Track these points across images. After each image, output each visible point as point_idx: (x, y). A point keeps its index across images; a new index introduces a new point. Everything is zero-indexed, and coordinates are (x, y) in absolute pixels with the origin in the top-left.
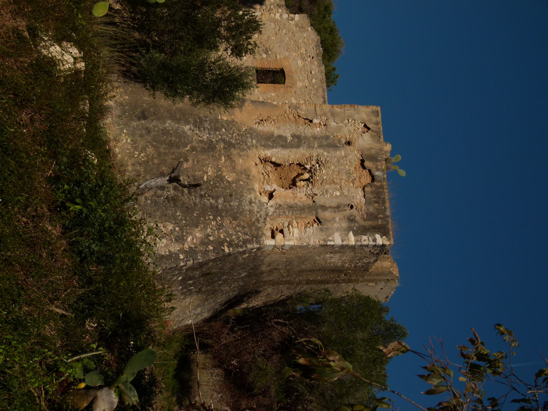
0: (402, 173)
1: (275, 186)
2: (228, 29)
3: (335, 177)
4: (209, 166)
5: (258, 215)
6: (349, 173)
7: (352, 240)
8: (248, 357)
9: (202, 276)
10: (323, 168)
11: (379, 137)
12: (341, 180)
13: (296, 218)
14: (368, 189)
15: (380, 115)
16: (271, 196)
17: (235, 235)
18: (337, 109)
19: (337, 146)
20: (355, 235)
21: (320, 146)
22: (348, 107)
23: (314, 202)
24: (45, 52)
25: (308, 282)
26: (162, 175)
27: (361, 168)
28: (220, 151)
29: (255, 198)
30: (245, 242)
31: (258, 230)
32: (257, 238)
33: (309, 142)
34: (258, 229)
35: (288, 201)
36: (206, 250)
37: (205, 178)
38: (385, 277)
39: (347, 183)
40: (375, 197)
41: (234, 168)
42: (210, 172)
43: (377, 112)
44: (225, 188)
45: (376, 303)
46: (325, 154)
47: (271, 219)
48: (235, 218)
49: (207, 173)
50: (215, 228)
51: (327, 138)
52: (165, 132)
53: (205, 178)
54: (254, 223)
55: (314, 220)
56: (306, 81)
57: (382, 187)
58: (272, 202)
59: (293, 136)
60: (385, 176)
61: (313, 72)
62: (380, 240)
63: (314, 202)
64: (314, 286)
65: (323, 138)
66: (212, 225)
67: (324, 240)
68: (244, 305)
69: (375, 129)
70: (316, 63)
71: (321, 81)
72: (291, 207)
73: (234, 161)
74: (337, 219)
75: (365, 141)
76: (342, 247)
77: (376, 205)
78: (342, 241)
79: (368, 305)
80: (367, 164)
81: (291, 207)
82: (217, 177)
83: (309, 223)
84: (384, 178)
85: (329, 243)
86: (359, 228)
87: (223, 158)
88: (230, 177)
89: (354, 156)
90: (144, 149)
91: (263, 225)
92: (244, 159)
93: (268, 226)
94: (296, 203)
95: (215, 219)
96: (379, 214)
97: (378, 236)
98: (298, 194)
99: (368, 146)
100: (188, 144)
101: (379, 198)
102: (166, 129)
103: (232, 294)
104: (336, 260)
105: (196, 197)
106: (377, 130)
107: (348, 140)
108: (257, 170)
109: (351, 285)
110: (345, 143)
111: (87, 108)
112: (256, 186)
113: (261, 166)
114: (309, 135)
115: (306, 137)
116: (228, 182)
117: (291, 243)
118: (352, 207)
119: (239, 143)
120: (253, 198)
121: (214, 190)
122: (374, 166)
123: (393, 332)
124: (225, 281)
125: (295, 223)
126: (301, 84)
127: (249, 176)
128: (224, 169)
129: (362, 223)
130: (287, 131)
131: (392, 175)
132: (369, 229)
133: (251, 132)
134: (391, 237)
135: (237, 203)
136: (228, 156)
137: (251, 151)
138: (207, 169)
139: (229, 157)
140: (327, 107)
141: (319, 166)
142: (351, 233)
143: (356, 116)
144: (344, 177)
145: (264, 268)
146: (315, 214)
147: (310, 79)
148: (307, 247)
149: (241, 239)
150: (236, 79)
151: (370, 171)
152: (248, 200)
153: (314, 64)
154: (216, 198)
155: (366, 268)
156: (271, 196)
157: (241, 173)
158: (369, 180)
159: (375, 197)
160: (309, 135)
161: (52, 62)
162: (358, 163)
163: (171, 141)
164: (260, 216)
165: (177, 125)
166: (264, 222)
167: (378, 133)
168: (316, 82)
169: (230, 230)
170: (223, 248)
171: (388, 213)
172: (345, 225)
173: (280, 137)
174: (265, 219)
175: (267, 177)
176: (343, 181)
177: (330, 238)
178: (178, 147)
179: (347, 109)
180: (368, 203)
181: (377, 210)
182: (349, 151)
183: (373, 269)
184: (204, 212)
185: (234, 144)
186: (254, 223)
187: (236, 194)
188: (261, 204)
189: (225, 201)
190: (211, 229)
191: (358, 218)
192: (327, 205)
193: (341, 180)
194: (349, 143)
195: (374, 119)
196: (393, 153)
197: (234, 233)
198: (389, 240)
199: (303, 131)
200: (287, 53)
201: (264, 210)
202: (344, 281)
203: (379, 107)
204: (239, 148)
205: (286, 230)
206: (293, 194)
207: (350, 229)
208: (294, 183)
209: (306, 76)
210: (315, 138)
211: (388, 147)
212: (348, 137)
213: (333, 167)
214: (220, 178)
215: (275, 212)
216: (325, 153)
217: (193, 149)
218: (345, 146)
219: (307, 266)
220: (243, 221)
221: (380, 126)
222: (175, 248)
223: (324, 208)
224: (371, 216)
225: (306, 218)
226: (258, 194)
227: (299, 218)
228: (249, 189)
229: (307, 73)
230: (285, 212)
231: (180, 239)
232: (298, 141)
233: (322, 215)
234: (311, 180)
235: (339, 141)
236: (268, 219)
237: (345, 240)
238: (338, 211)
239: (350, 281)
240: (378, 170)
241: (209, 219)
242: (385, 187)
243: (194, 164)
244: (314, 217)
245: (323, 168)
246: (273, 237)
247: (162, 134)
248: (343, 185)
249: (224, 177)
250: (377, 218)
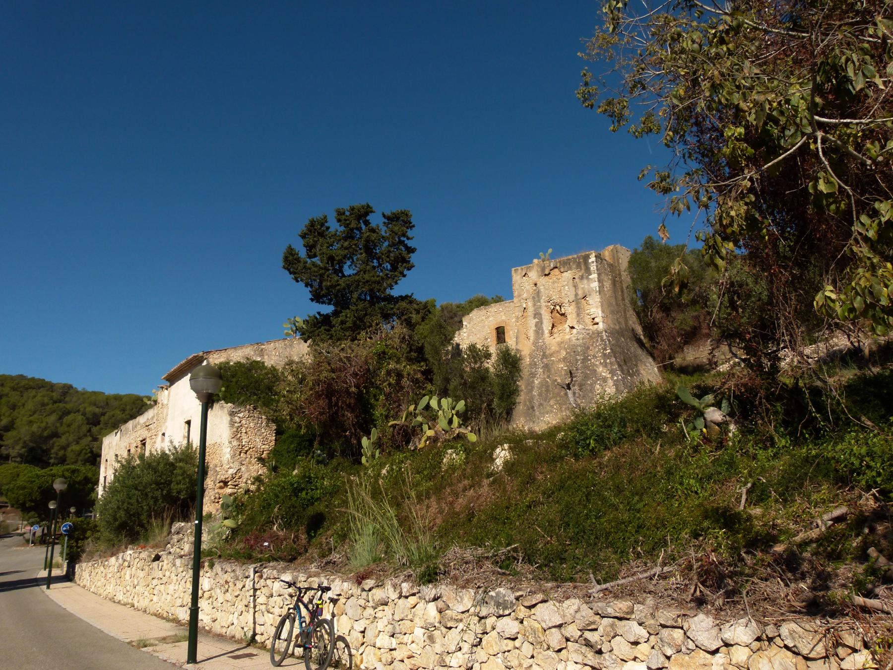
0: (550, 251)
1: (566, 326)
2: (476, 362)
6: (554, 283)
7: (594, 276)
8: (675, 331)
9: (626, 364)
14: (562, 270)
16: (572, 328)
18: (516, 294)
22: (514, 288)
24: (500, 468)
25: (623, 299)
26: (566, 394)
30: (602, 340)
32: (599, 333)
34: (593, 333)
38: (615, 253)
45: (632, 257)
46: (544, 298)
48: (588, 348)
51: (534, 298)
52: (540, 394)
57: (560, 262)
59: (535, 318)
62: (592, 259)
64: (626, 296)
68: (642, 337)
72: (578, 315)
75: (533, 275)
76: (599, 281)
79: (634, 262)
80: (547, 273)
89: (543, 281)
90: (552, 406)
93: (591, 327)
97: (590, 261)
103: (636, 345)
104: (608, 284)
108: (558, 338)
109: (622, 273)
111: (531, 441)
112: (568, 337)
113: (555, 336)
117: (600, 312)
123: (650, 245)
124: (628, 350)
129: (583, 271)
130: (532, 322)
131: (552, 257)
133: (535, 343)
139: (551, 355)
140: (515, 300)
145: (617, 327)
146: (580, 300)
148: (602, 303)
150: (504, 355)
154: (577, 360)
155: (611, 266)
156: (572, 328)
158: (556, 270)
161: (506, 463)
169: (596, 350)
171: (575, 256)
172: (585, 281)
173: (536, 326)
178: (548, 386)
180: (570, 269)
183: (611, 261)
184: (587, 367)
188: (578, 333)
194: (536, 285)
195: (520, 271)
196: (539, 258)
202: (620, 278)
207: (587, 278)
208: (563, 315)
210: (534, 305)
211: (536, 261)
217: (549, 377)
219: (613, 301)
222: (610, 382)
223: (576, 295)
224: (578, 266)
231: (605, 380)
232: (537, 315)
233: (581, 295)
239: (620, 274)
248: (561, 285)
250: (579, 263)
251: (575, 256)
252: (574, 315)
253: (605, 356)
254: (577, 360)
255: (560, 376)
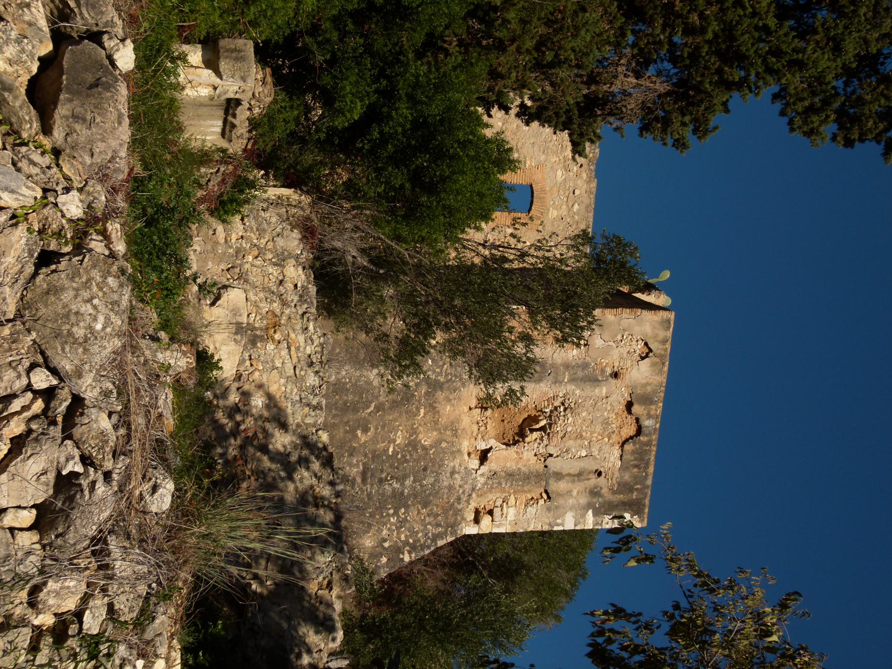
1: (493, 442)
3: (584, 428)
4: (398, 430)
5: (461, 491)
6: (606, 423)
10: (569, 415)
11: (663, 364)
12: (592, 433)
13: (515, 492)
15: (671, 329)
16: (484, 456)
17: (422, 531)
19: (597, 380)
20: (595, 514)
21: (572, 380)
23: (546, 466)
27: (626, 412)
28: (419, 401)
29: (460, 465)
31: (456, 515)
33: (557, 374)
35: (508, 465)
36: (376, 566)
37: (391, 449)
39: (600, 437)
40: (635, 459)
41: (436, 423)
42: (400, 438)
43: (669, 321)
44: (418, 461)
46: (576, 392)
47: (478, 496)
48: (425, 505)
49: (395, 441)
50: (394, 527)
51: (585, 366)
53: (391, 449)
54: (453, 505)
55: (541, 494)
56: (564, 207)
58: (484, 469)
60: (658, 426)
61: (577, 192)
63: (546, 466)
65: (579, 366)
66: (392, 524)
67: (550, 524)
69: (659, 352)
70: (584, 175)
71: (587, 207)
72: (511, 475)
73: (438, 412)
74: (575, 493)
77: (635, 470)
78: (575, 525)
80: (636, 409)
81: (511, 475)
82: (409, 444)
83: (532, 498)
84: (655, 429)
85: (556, 528)
86: (602, 505)
87: (422, 411)
88: (426, 439)
89: (619, 393)
91: (466, 504)
92: (453, 405)
94: (519, 469)
95: (396, 513)
96: (636, 483)
98: (525, 453)
99: (644, 381)
100: (371, 402)
101: (642, 459)
102: (340, 382)
105: (372, 485)
106: (663, 352)
107: (616, 369)
110: (611, 375)
114: (559, 361)
115: (553, 366)
116: (425, 448)
118: (600, 474)
119: (451, 379)
120: (457, 466)
121: (401, 468)
122: (646, 412)
125: (512, 500)
126: (555, 213)
127: (456, 430)
128: (421, 428)
132: (617, 506)
134: (646, 516)
135: (433, 479)
136: (431, 405)
137: (466, 389)
138: (395, 434)
141: (565, 410)
142: (590, 512)
143: (637, 329)
144: (599, 428)
146: (542, 484)
147: (571, 204)
149: (430, 535)
151: (637, 420)
152: (449, 470)
153: (582, 178)
154: (401, 479)
157: (446, 429)
159: (635, 459)
160: (559, 361)
162: (622, 407)
163: (345, 403)
164: (463, 492)
165: (358, 373)
166: (468, 502)
167: (661, 357)
168: (578, 210)
170: (401, 556)
174: (470, 495)
175: (482, 428)
176: (595, 435)
177: (559, 521)
178: (356, 410)
179: (624, 316)
180: (623, 468)
181: (635, 477)
182: (614, 388)
184: (381, 508)
185: (442, 384)
186: (453, 505)
187: (433, 465)
188: (468, 472)
189: (414, 481)
190: (389, 529)
191: (605, 491)
192: (565, 472)
193: (592, 433)
194: (616, 375)
197: (422, 528)
198: (642, 521)
199: (551, 354)
200: (543, 157)
201: (470, 481)
203: (673, 313)
204: (449, 389)
205: (497, 512)
206: (517, 453)
207: (589, 506)
209: (565, 199)
210: (567, 366)
212: (616, 364)
213: (584, 414)
214: (413, 444)
215: (486, 483)
216: (578, 392)
217: (378, 408)
218: (610, 379)
220: (437, 506)
221: (668, 346)
223: (559, 476)
224: (624, 487)
225: (530, 491)
226: (466, 457)
227: (519, 491)
228: (453, 453)
229: (567, 193)
230: (500, 484)
234: (549, 431)
235: (603, 371)
236: (474, 495)
237: (579, 523)
238: (579, 480)
240: (649, 416)
241: (388, 515)
242: (654, 443)
243: (376, 433)
244: (543, 490)
245: (569, 415)
246: (477, 521)
247: (333, 392)
249: (420, 441)
250: (631, 490)
251: (649, 482)
252: (511, 466)
253: (397, 550)
254: (401, 479)
255: (374, 440)
